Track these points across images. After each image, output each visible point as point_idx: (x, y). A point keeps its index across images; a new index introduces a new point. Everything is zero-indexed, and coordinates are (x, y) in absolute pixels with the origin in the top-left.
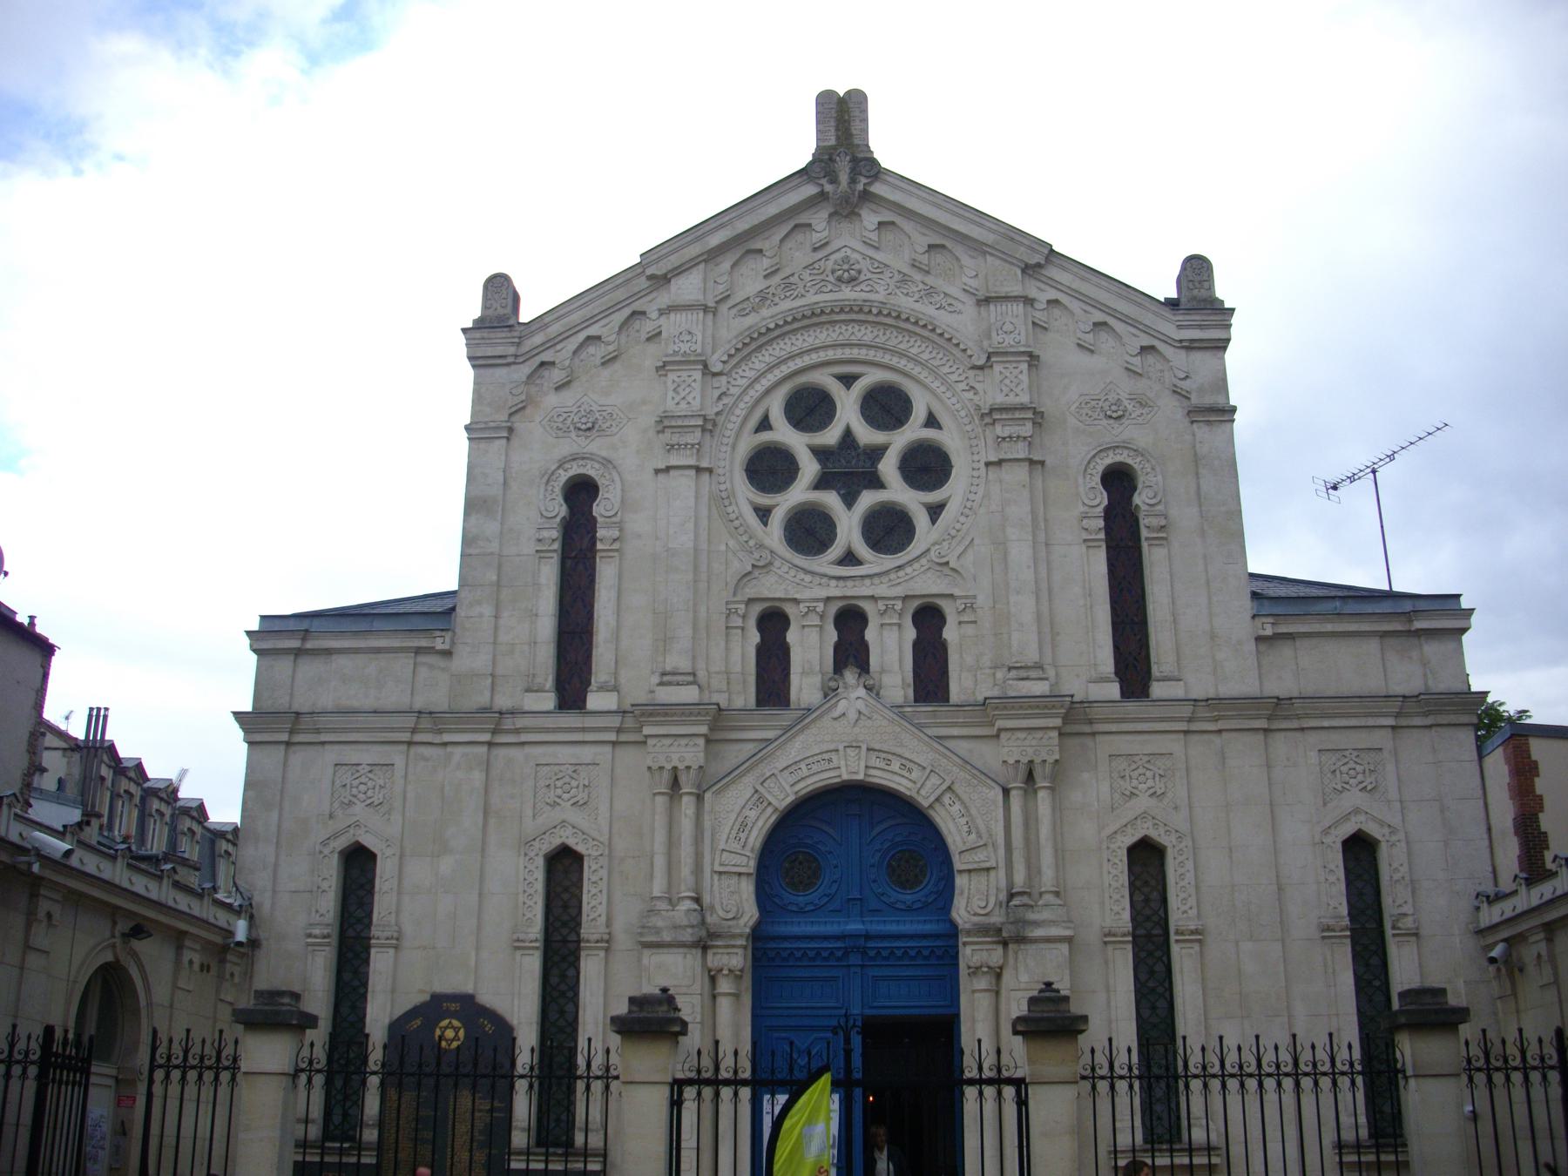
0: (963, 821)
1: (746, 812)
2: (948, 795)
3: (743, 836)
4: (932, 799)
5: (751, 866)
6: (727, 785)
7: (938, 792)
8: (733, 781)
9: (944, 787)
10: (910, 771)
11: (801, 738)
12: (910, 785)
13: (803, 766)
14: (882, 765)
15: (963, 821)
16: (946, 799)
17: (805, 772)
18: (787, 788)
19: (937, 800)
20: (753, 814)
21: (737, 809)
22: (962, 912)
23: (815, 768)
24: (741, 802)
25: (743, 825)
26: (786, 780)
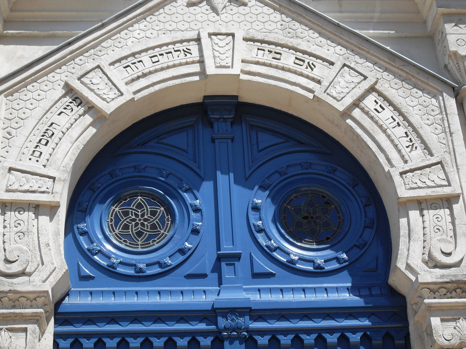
0: (400, 131)
1: (56, 118)
2: (372, 97)
3: (46, 150)
4: (348, 101)
5: (61, 195)
6: (24, 83)
7: (358, 92)
8: (34, 78)
9: (366, 85)
10: (311, 66)
11: (142, 25)
12: (311, 85)
13: (145, 57)
14: (268, 58)
15: (400, 131)
16: (370, 102)
17: (148, 65)
18: (123, 88)
19: (356, 104)
20: (63, 121)
21: (39, 112)
22: (416, 261)
23: (164, 61)
24: (46, 104)
25: (46, 137)
26: (119, 75)
